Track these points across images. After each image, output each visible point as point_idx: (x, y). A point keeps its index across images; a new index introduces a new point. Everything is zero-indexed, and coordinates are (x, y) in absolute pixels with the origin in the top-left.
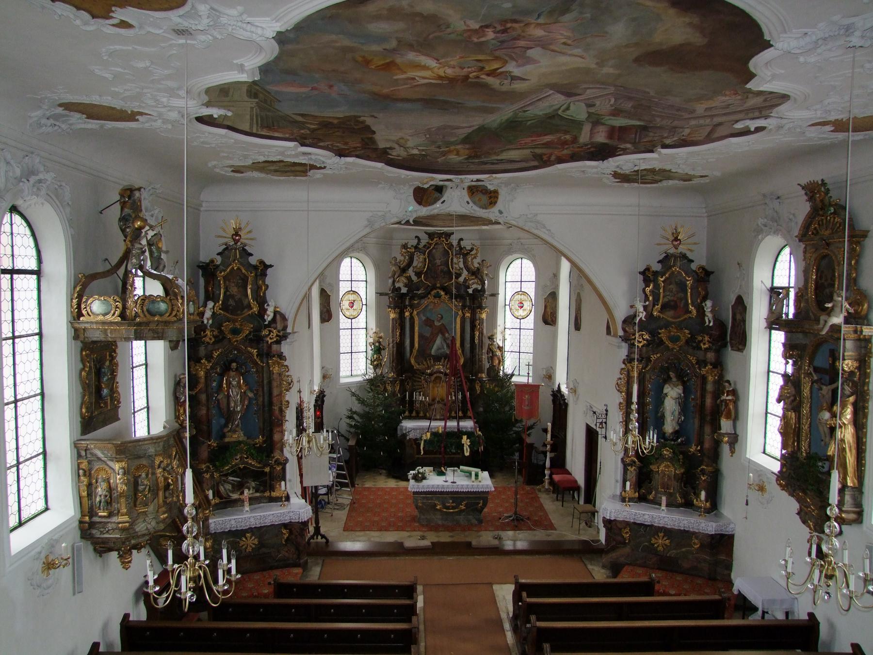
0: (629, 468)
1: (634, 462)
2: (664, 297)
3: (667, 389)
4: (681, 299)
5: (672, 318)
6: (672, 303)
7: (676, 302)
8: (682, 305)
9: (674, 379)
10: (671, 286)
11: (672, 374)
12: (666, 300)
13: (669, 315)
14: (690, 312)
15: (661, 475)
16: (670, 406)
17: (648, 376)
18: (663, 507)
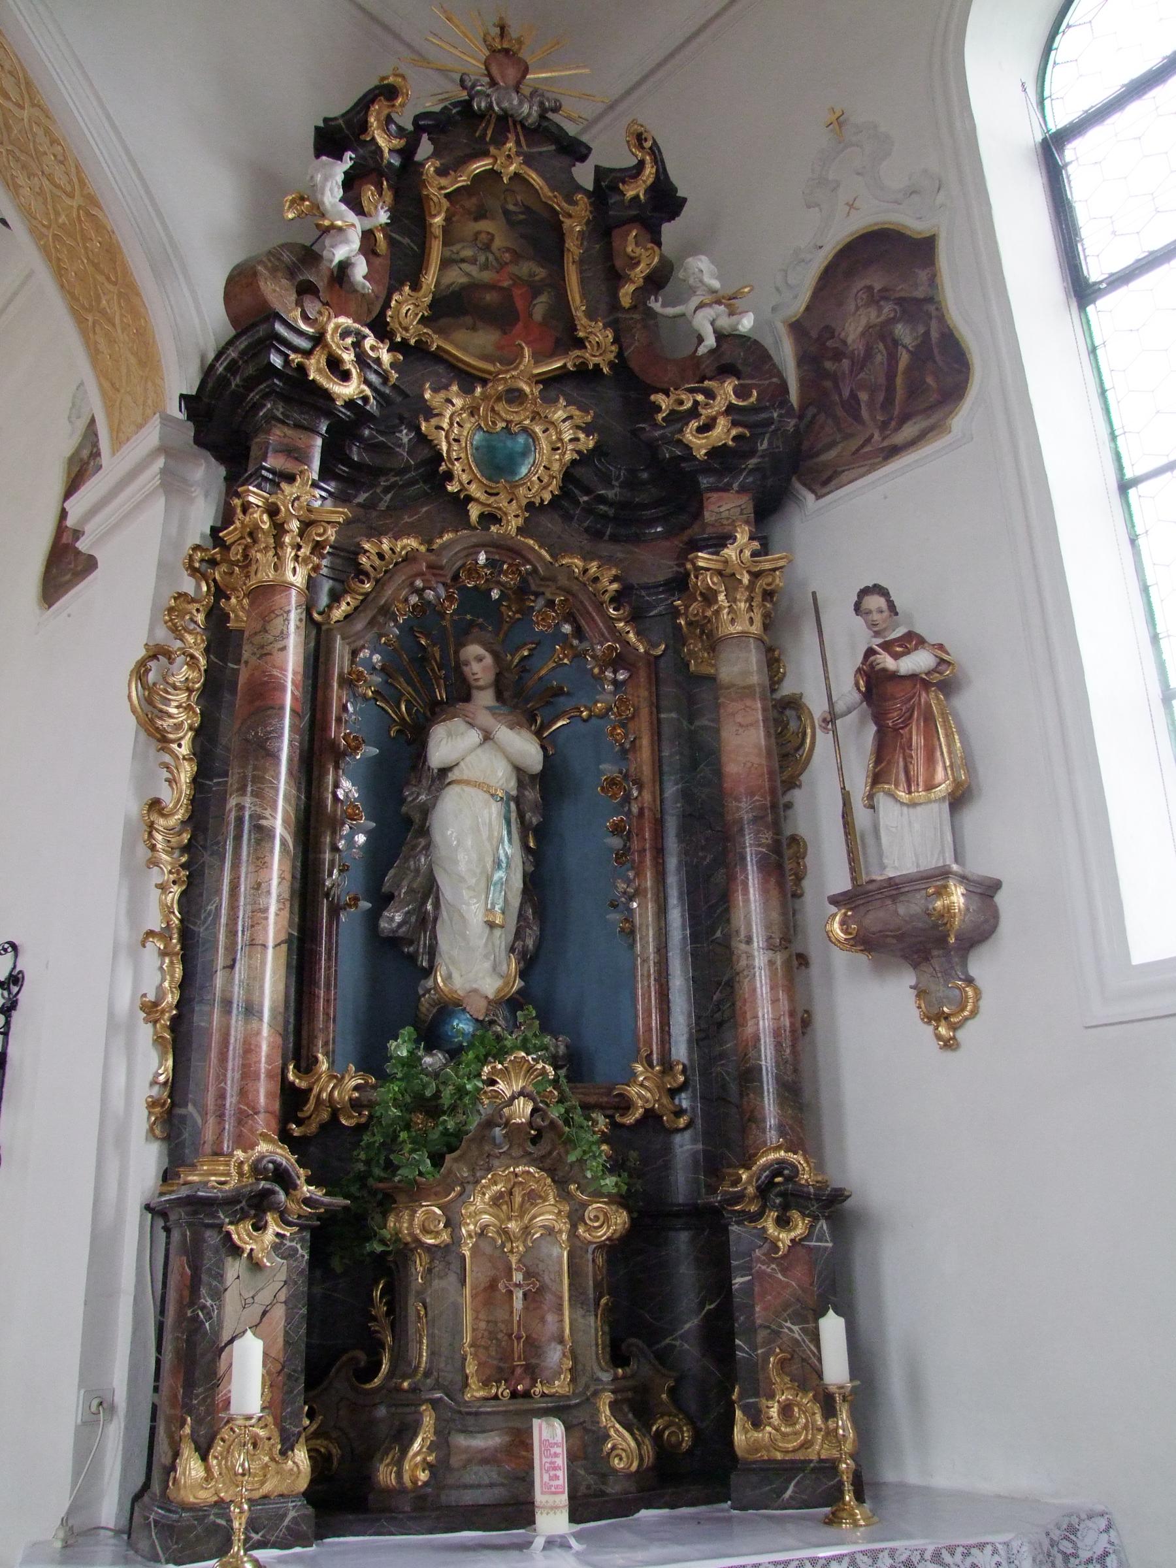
0: (241, 1233)
1: (282, 1177)
2: (445, 263)
3: (449, 743)
4: (535, 291)
5: (485, 358)
6: (490, 297)
7: (507, 293)
8: (539, 312)
9: (485, 698)
10: (485, 225)
11: (478, 662)
12: (456, 277)
13: (468, 345)
14: (580, 344)
15: (475, 1274)
16: (474, 845)
17: (340, 649)
18: (553, 1519)
